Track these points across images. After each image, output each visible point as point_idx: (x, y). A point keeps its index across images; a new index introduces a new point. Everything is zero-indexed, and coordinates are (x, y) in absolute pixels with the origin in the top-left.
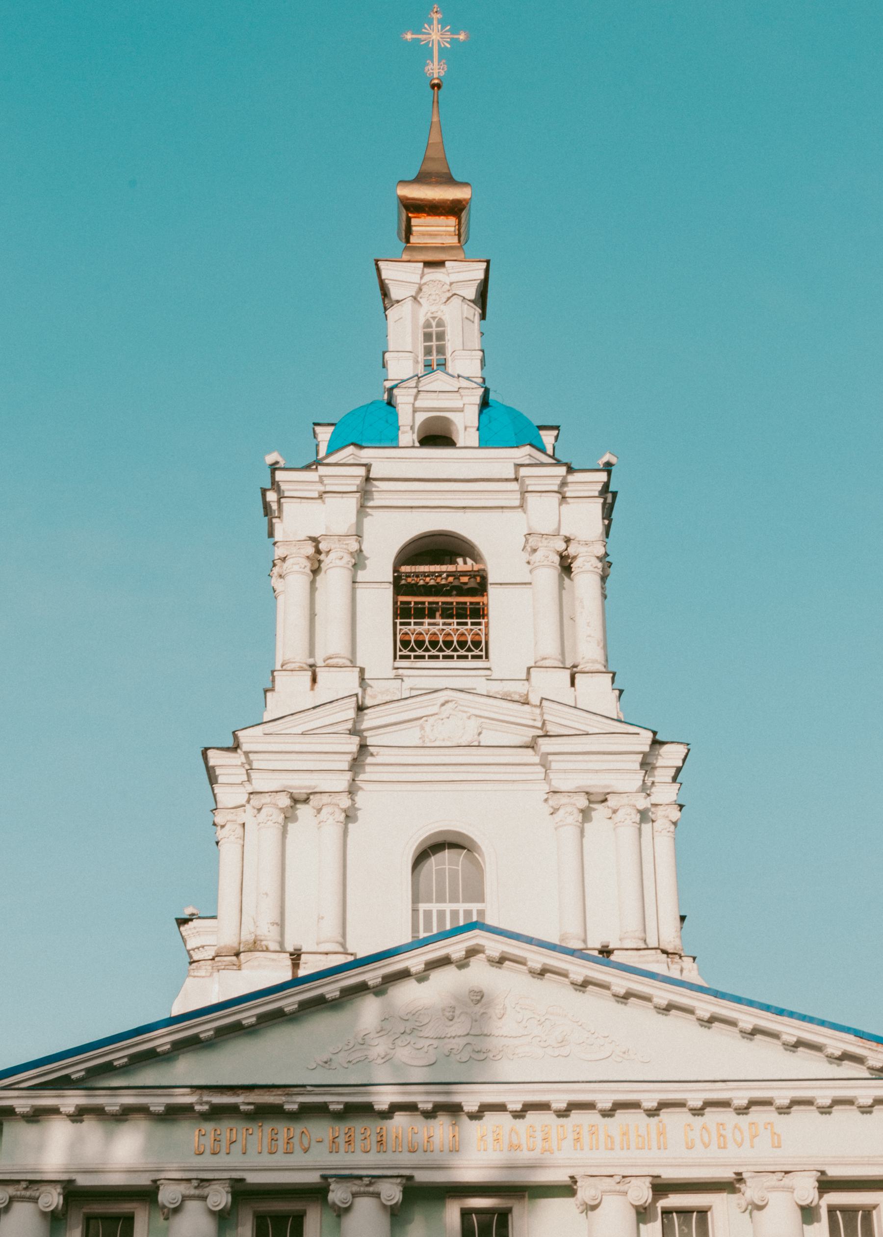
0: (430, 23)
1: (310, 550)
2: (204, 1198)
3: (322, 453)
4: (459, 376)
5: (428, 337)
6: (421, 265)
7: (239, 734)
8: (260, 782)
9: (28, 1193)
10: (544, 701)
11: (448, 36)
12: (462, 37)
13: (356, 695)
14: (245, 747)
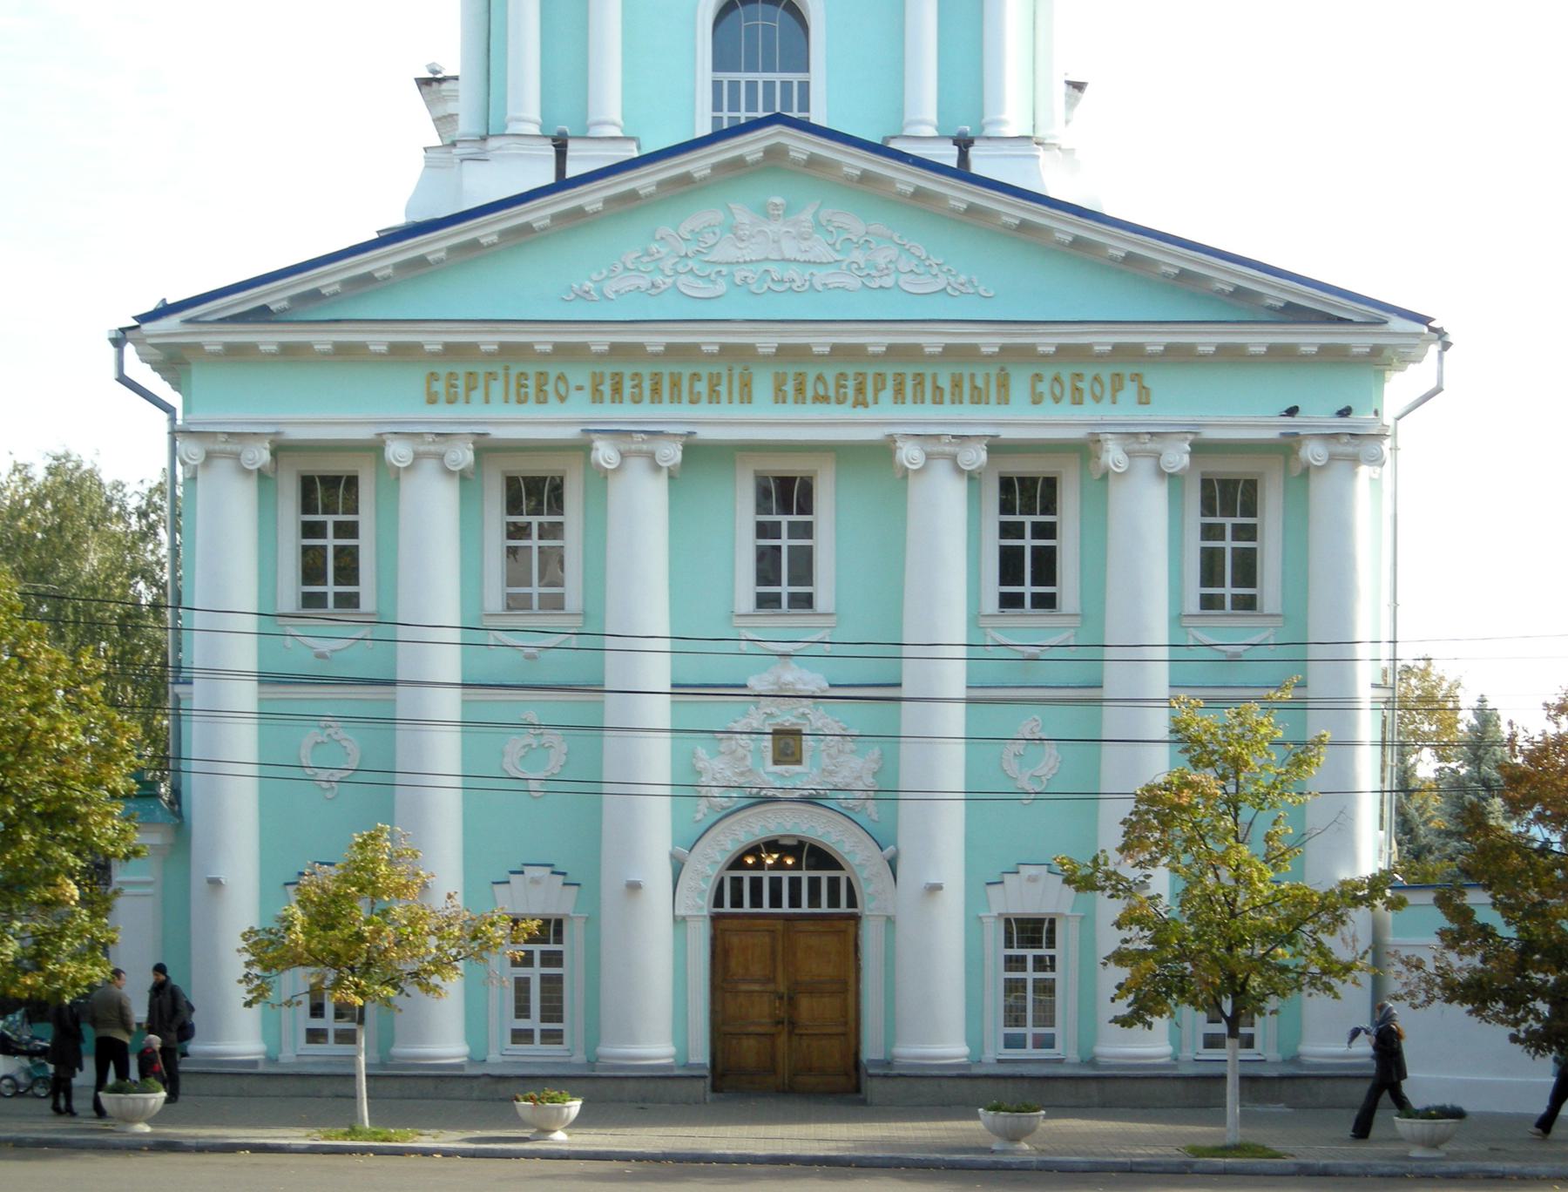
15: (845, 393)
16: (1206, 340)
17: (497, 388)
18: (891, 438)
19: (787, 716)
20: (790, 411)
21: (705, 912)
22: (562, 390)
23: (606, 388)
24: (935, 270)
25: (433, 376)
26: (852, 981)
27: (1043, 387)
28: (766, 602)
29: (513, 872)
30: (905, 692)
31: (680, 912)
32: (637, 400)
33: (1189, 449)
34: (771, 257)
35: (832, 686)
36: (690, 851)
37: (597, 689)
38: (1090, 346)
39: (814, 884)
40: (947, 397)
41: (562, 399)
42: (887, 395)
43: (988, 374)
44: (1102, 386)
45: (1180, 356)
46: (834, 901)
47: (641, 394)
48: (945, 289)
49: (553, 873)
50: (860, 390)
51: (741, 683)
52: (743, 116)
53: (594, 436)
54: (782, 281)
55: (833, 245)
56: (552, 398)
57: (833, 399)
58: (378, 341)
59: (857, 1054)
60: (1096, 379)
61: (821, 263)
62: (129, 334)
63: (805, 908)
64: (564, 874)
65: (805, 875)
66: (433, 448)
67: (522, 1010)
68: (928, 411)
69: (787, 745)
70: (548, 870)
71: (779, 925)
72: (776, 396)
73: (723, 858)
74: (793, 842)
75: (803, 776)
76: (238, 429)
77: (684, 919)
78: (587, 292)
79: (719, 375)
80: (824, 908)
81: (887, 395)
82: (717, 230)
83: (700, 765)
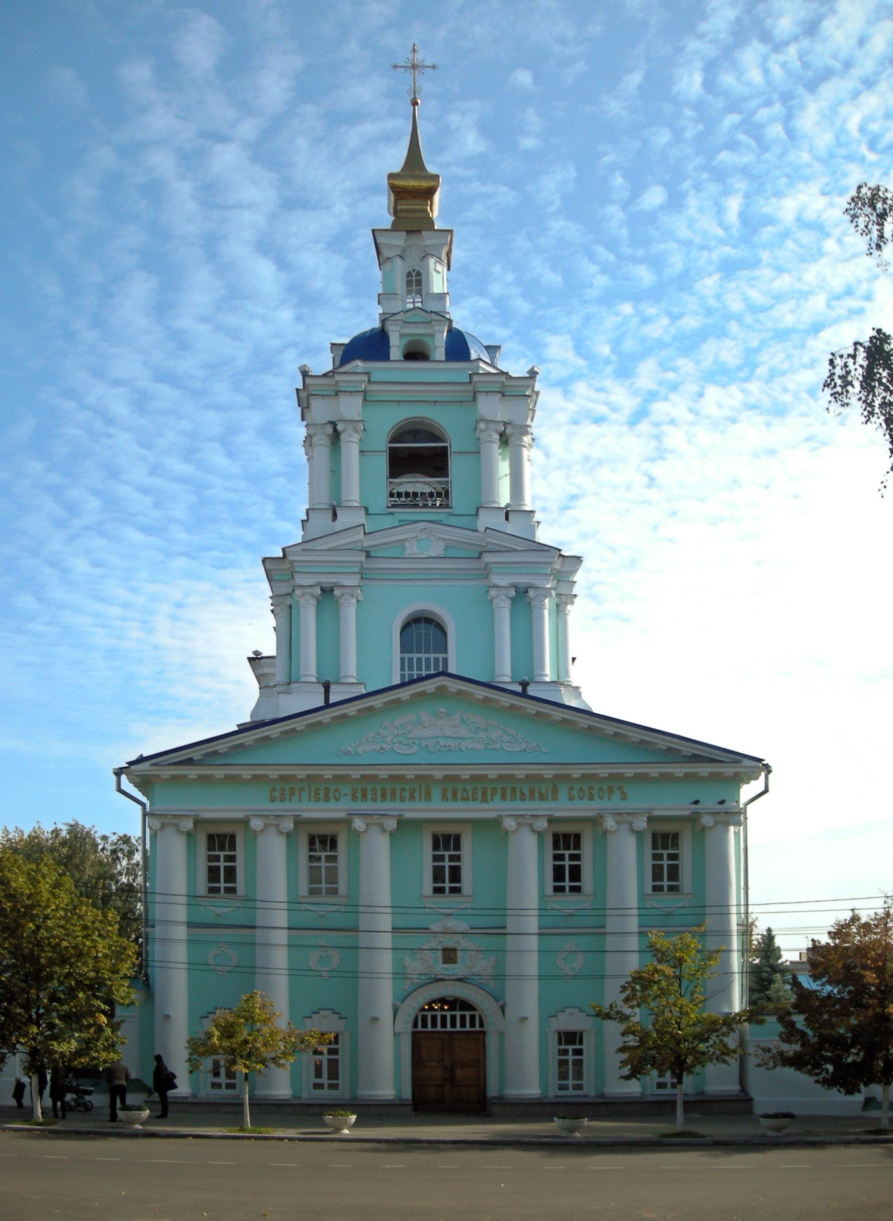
1: (330, 430)
3: (338, 363)
4: (431, 312)
7: (287, 550)
8: (300, 580)
10: (488, 531)
13: (363, 525)
14: (291, 558)
15: (477, 797)
16: (654, 771)
17: (305, 795)
18: (501, 817)
19: (449, 942)
20: (450, 805)
22: (337, 795)
23: (359, 795)
24: (520, 741)
25: (273, 790)
27: (574, 793)
28: (438, 891)
30: (508, 931)
31: (397, 1030)
32: (374, 800)
33: (646, 819)
34: (440, 735)
35: (471, 928)
36: (402, 1002)
37: (356, 930)
38: (597, 774)
39: (463, 1018)
40: (527, 798)
41: (337, 800)
42: (497, 797)
43: (547, 788)
44: (603, 792)
45: (642, 779)
46: (473, 1025)
47: (376, 798)
48: (525, 750)
49: (334, 1013)
50: (484, 795)
51: (426, 927)
52: (424, 673)
53: (353, 816)
54: (445, 746)
55: (470, 730)
56: (332, 799)
57: (471, 799)
58: (247, 774)
59: (485, 1094)
60: (600, 789)
61: (464, 738)
62: (123, 770)
63: (458, 1028)
64: (339, 1013)
65: (458, 1014)
66: (274, 822)
67: (318, 1074)
68: (518, 804)
69: (449, 955)
70: (331, 1012)
72: (443, 798)
74: (452, 999)
75: (458, 969)
76: (177, 813)
77: (399, 1034)
78: (349, 752)
79: (414, 789)
81: (497, 797)
82: (413, 724)
83: (406, 964)
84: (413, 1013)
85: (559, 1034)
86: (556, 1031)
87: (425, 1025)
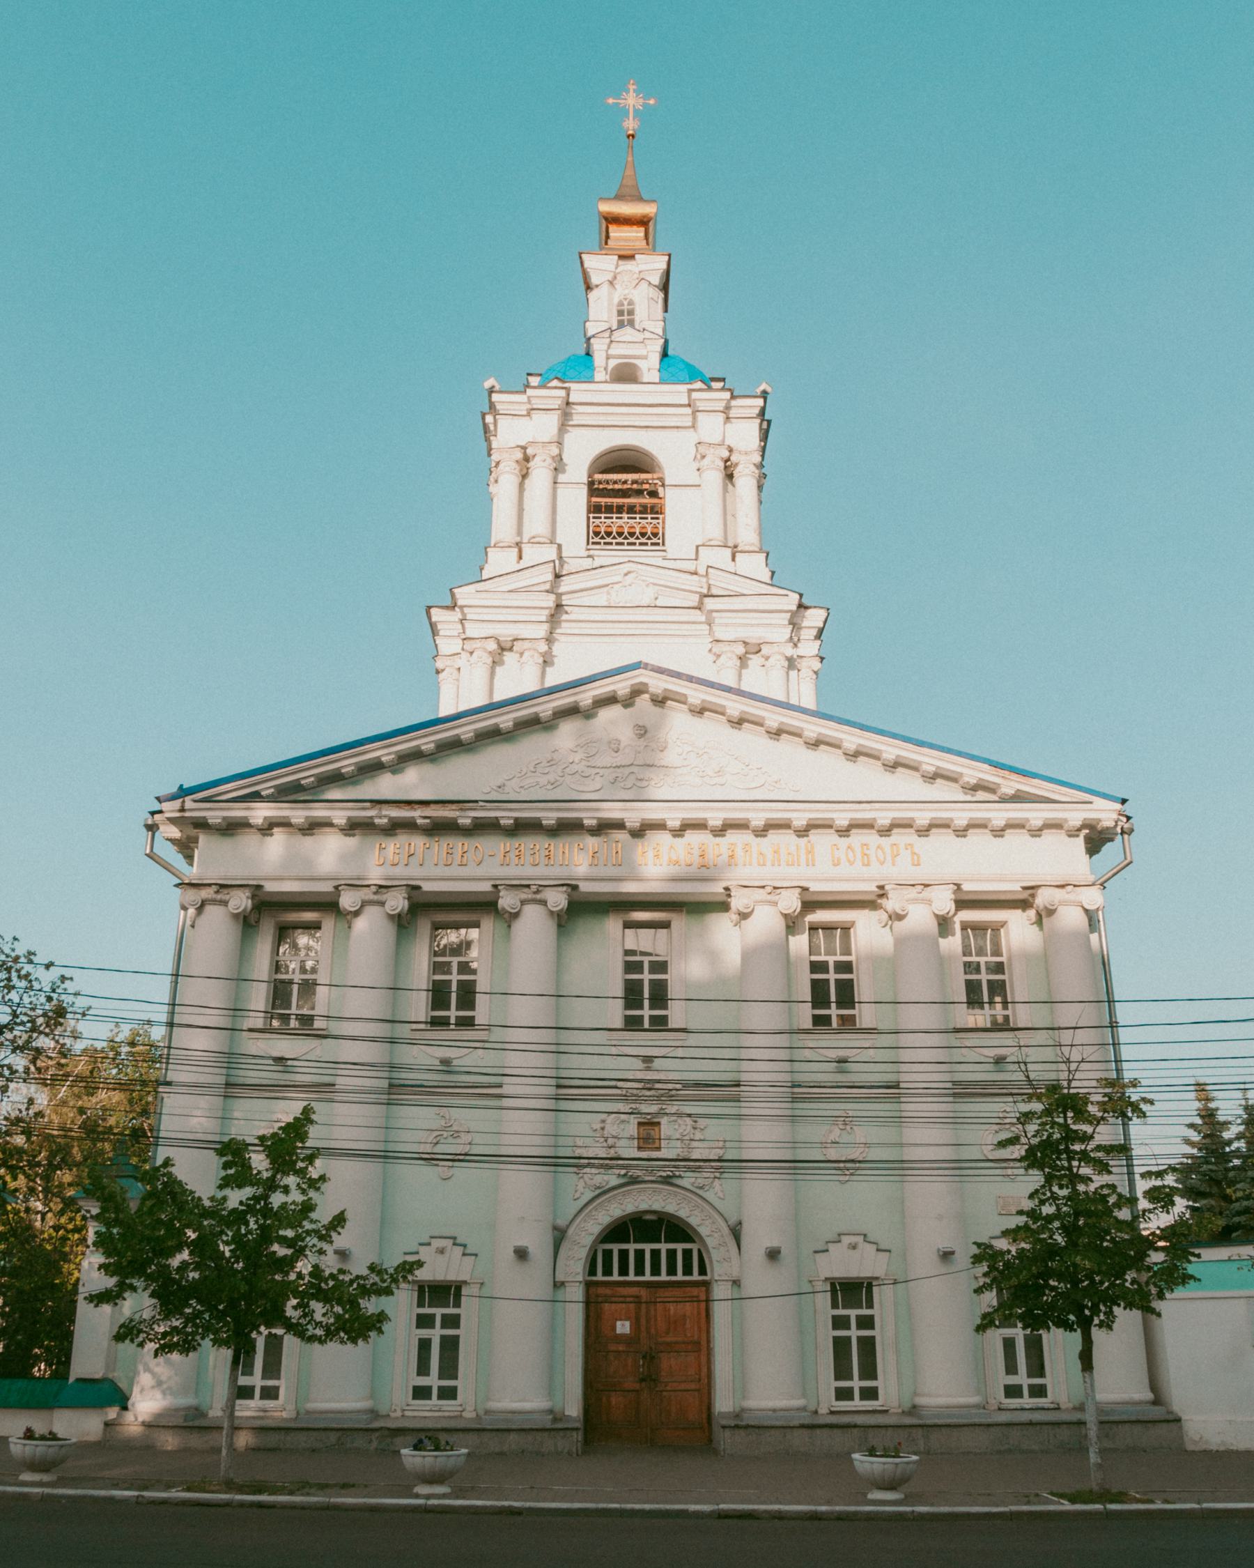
0: (628, 92)
2: (382, 904)
5: (620, 313)
6: (616, 257)
9: (219, 897)
11: (641, 101)
12: (652, 102)
21: (580, 1278)
26: (704, 1343)
29: (421, 1244)
31: (560, 1277)
46: (688, 1270)
63: (664, 1277)
64: (465, 1246)
65: (663, 1247)
67: (423, 1369)
71: (643, 1293)
73: (596, 1230)
77: (563, 1284)
80: (680, 1277)
84: (588, 1241)
85: (833, 1285)
86: (827, 1279)
87: (608, 1271)
